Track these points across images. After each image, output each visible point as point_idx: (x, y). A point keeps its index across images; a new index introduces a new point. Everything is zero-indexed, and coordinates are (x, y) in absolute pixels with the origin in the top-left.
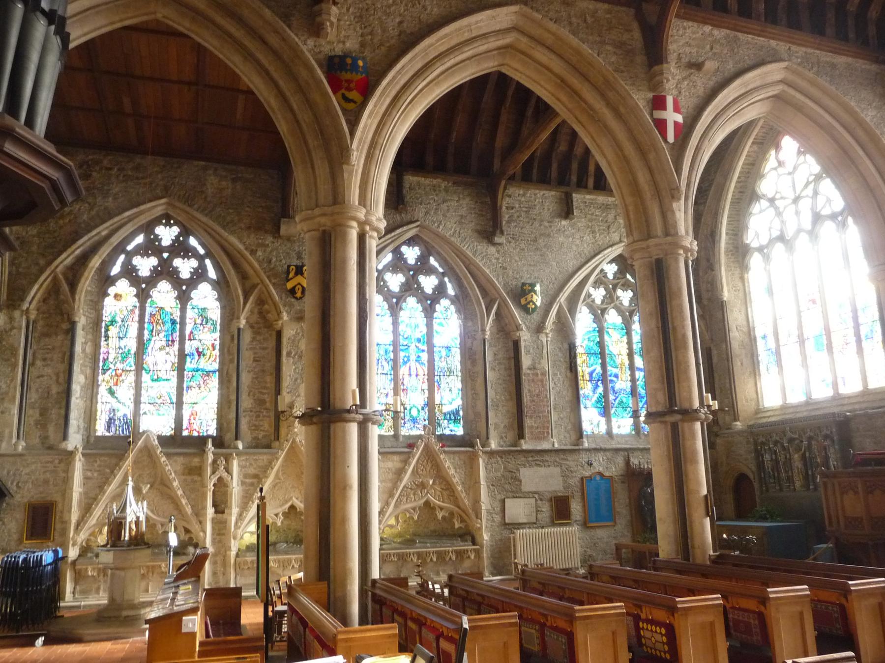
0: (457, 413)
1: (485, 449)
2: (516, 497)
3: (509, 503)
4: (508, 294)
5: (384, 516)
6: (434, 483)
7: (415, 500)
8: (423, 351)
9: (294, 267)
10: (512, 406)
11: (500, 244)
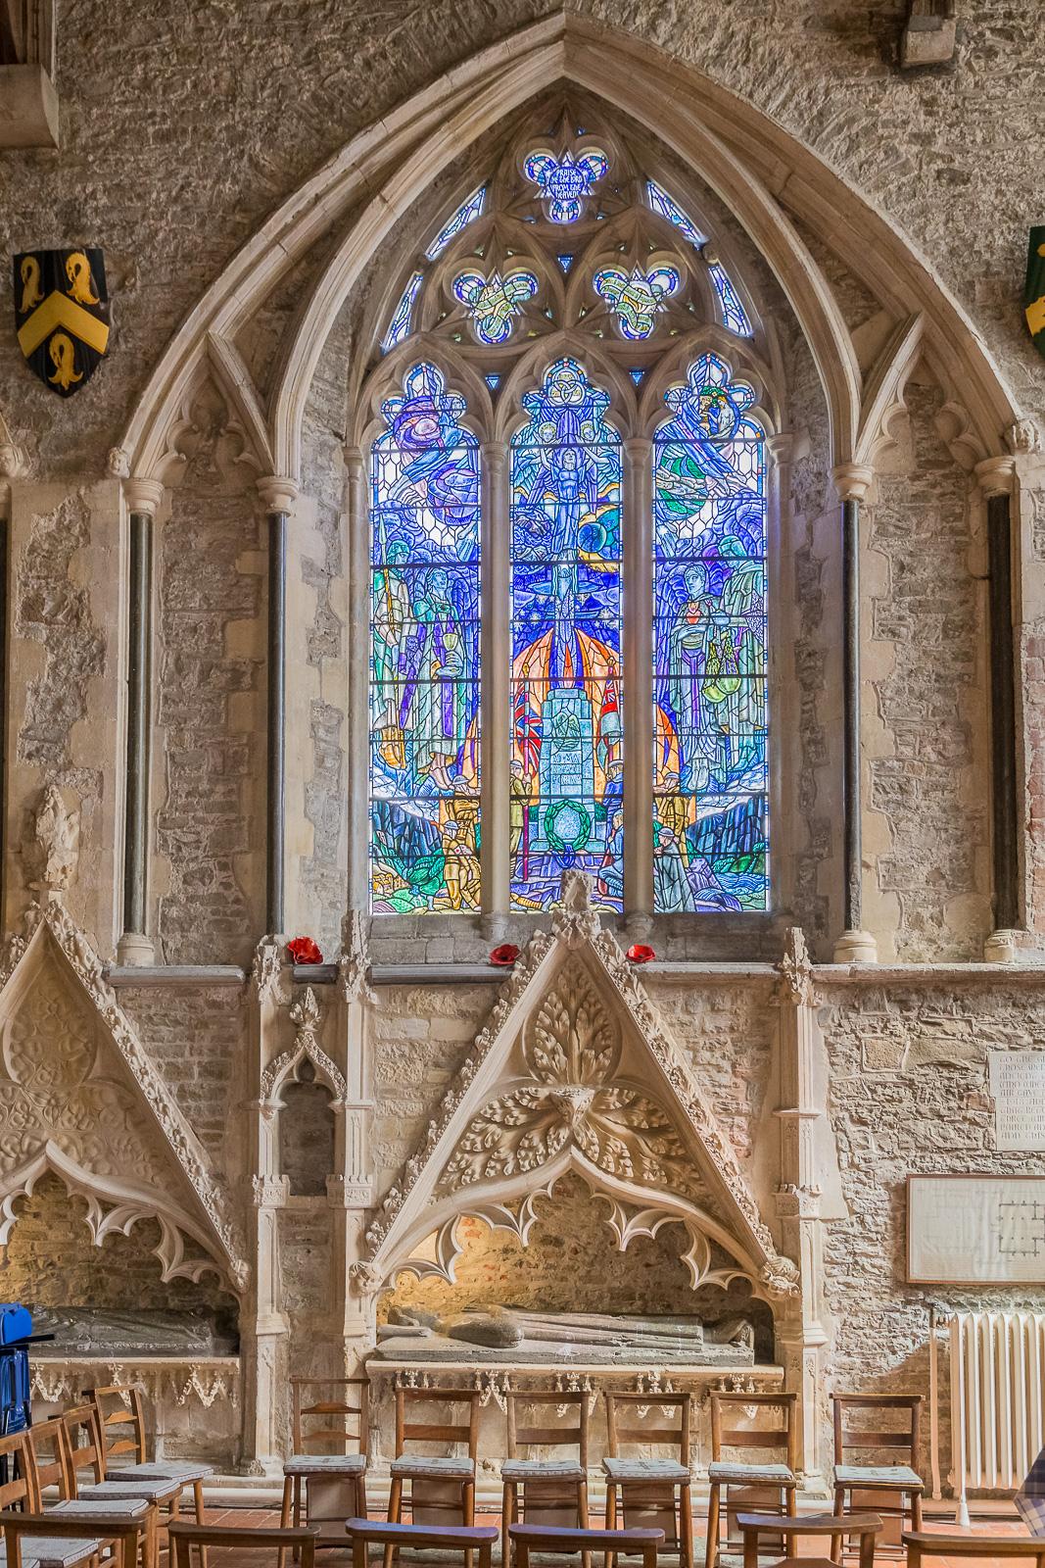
0: (748, 821)
1: (824, 967)
2: (967, 1174)
3: (922, 1193)
4: (966, 291)
5: (386, 1223)
6: (599, 1104)
7: (518, 1166)
8: (610, 579)
9: (32, 262)
10: (973, 785)
11: (939, 68)
